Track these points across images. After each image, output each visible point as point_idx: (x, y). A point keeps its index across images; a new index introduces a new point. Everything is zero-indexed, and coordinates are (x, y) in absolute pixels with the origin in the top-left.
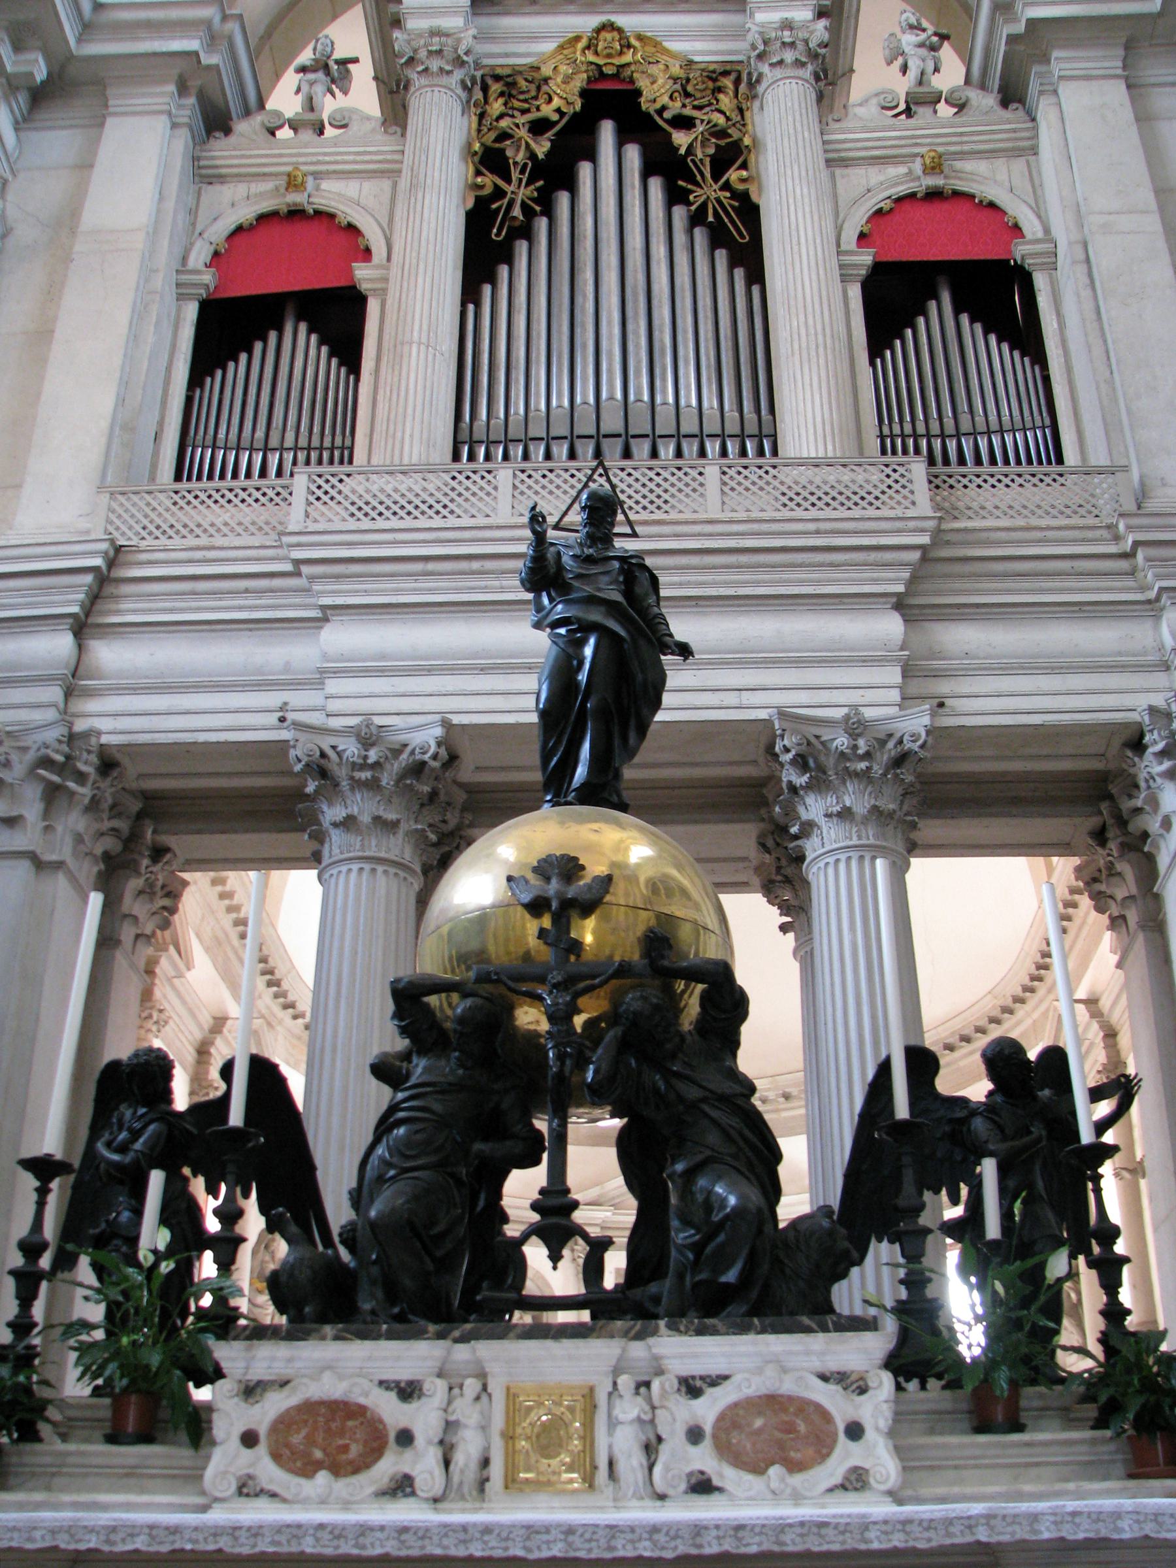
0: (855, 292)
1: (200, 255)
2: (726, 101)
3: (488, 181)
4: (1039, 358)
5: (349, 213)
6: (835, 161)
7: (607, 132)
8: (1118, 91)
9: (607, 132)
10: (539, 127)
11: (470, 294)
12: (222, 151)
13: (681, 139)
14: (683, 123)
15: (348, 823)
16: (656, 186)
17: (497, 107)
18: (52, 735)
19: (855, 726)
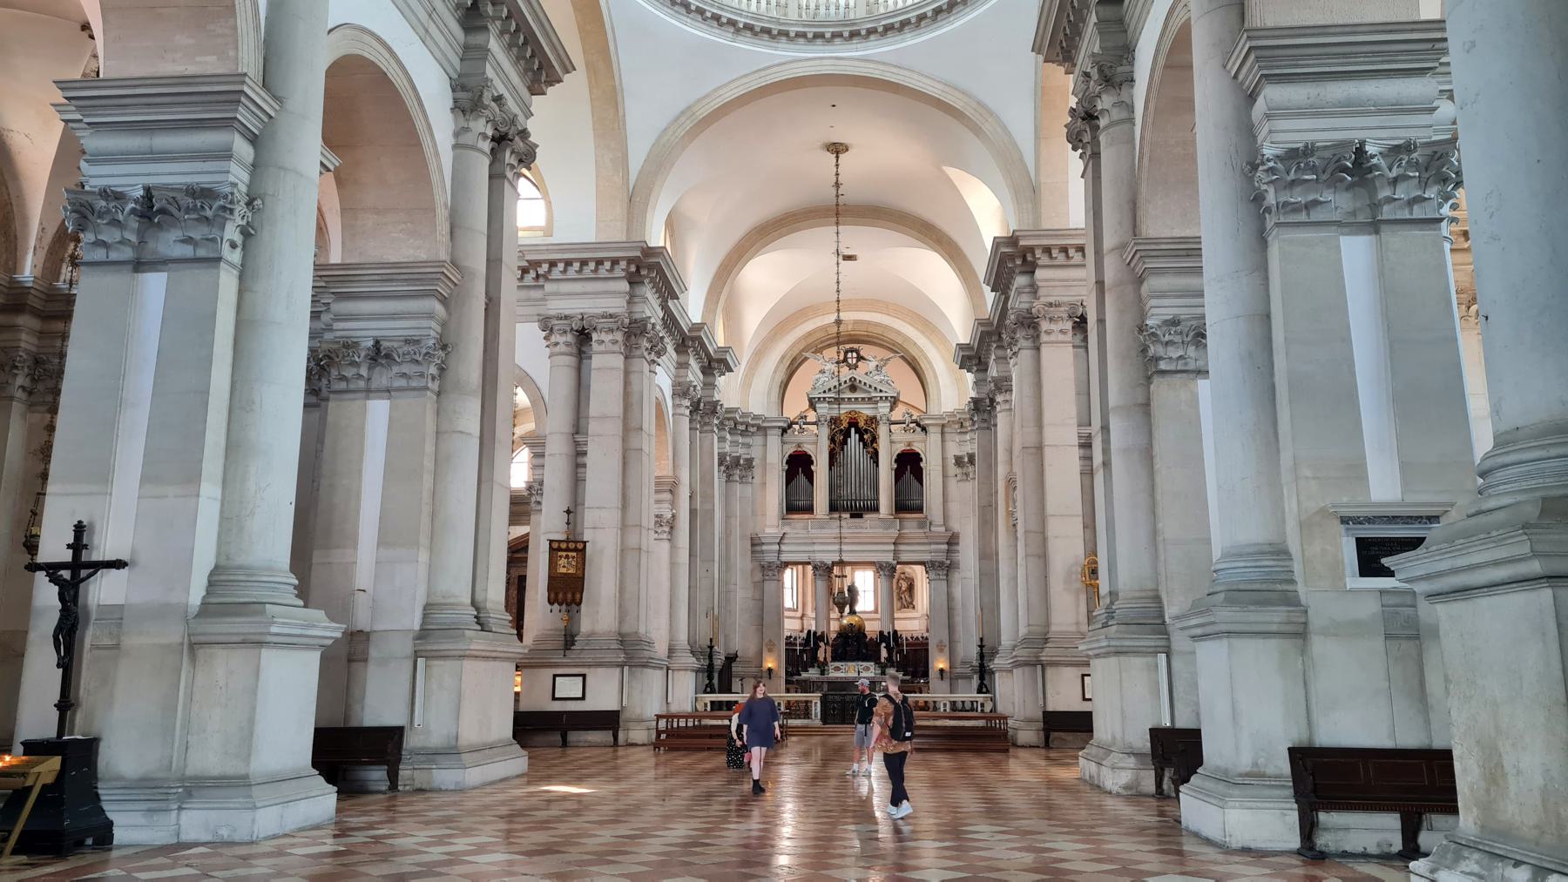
0: (893, 472)
2: (874, 426)
3: (832, 445)
4: (922, 484)
5: (810, 453)
6: (892, 442)
7: (853, 430)
8: (940, 435)
9: (853, 430)
10: (841, 430)
11: (830, 469)
13: (865, 437)
14: (866, 431)
15: (820, 575)
16: (861, 443)
17: (833, 427)
18: (779, 563)
19: (887, 563)
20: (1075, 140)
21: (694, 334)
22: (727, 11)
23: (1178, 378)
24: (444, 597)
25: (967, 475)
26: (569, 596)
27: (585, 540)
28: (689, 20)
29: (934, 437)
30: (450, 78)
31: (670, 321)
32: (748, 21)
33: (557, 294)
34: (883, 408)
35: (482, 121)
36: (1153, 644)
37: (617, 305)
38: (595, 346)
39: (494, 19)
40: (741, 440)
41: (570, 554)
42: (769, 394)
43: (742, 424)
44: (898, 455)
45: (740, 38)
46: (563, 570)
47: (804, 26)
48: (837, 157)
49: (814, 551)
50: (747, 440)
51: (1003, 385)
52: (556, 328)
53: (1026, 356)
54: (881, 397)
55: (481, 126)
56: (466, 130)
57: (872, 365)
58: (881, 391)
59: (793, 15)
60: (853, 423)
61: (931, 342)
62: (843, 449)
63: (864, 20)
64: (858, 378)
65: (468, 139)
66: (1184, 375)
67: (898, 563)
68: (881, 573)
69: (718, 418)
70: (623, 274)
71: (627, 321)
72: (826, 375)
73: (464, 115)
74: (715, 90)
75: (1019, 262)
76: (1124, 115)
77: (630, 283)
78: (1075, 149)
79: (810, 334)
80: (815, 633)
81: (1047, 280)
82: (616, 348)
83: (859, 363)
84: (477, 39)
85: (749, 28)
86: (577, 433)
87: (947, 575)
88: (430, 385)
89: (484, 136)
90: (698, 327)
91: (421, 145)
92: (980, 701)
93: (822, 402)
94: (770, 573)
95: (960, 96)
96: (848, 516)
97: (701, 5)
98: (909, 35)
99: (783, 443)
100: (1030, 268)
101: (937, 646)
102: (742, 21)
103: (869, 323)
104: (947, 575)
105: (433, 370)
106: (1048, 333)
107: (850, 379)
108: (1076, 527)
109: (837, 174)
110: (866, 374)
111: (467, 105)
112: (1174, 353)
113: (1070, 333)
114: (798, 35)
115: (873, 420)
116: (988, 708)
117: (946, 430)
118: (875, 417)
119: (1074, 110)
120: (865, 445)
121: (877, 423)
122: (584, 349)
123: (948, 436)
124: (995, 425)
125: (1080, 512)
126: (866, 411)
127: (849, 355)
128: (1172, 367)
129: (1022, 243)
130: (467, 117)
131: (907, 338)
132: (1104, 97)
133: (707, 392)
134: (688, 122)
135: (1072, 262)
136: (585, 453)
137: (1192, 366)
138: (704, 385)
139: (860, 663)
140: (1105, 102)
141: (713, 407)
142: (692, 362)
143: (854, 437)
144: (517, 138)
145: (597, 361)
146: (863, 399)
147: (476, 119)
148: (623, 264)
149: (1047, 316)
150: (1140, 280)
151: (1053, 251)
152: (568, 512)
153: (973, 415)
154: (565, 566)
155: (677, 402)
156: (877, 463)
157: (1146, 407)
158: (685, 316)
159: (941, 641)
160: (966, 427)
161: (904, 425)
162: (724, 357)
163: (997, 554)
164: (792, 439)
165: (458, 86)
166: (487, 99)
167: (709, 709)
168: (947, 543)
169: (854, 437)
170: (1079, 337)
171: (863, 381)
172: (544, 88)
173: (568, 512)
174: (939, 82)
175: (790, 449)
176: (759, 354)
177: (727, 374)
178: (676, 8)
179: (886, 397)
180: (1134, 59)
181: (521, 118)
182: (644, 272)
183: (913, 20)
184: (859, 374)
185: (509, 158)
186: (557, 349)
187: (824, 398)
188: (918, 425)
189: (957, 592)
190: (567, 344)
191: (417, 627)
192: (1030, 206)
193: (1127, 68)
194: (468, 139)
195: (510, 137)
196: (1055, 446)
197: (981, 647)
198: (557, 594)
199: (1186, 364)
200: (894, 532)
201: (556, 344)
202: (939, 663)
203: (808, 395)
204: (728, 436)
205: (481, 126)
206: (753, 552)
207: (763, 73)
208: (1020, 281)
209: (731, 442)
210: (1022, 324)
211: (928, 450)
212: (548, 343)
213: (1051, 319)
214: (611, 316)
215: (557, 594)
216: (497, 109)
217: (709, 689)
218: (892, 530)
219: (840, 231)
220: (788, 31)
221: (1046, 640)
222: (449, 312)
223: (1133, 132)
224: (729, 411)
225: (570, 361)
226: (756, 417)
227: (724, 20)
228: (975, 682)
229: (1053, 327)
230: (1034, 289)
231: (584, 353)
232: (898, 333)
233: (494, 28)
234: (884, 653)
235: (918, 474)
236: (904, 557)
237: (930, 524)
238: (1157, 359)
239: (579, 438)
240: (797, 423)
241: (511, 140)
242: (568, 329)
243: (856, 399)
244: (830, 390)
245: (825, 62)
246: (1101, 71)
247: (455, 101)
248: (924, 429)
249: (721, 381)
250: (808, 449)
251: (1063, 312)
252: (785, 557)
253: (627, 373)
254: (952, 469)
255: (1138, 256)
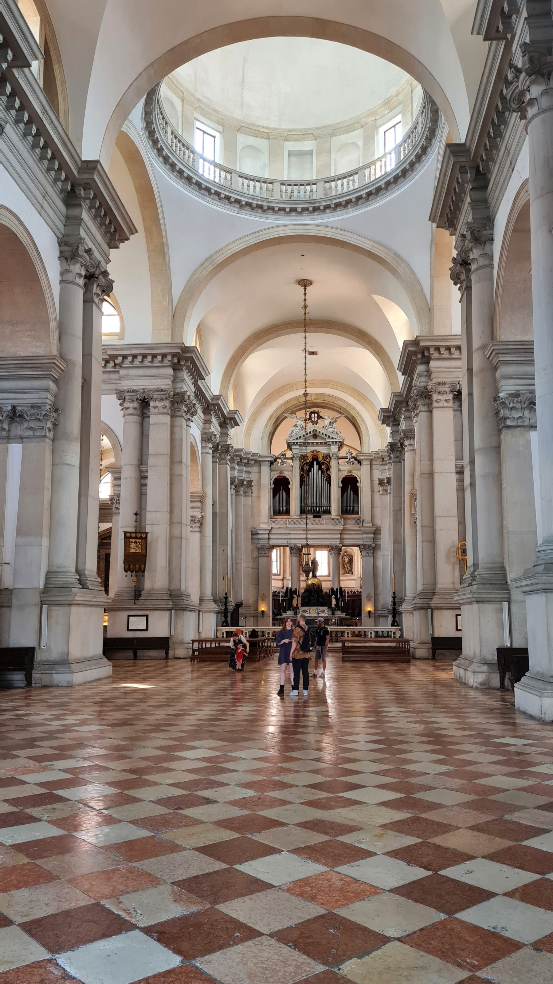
1: (272, 482)
2: (328, 460)
4: (358, 497)
5: (288, 477)
6: (339, 470)
7: (315, 463)
8: (369, 466)
9: (315, 463)
11: (301, 487)
12: (273, 467)
13: (323, 467)
14: (323, 463)
16: (320, 471)
18: (268, 546)
20: (456, 278)
21: (215, 402)
22: (234, 194)
23: (517, 431)
24: (58, 567)
25: (386, 491)
26: (137, 566)
27: (147, 531)
28: (210, 200)
29: (366, 467)
30: (58, 238)
31: (200, 394)
32: (248, 200)
33: (127, 376)
34: (334, 449)
35: (78, 266)
36: (499, 596)
37: (165, 384)
38: (152, 410)
39: (85, 199)
40: (244, 469)
41: (138, 540)
42: (262, 439)
43: (245, 459)
44: (343, 478)
45: (243, 211)
46: (134, 551)
47: (284, 203)
48: (305, 289)
49: (290, 539)
50: (249, 469)
51: (409, 434)
52: (127, 398)
53: (423, 416)
54: (333, 442)
55: (77, 268)
56: (68, 271)
57: (327, 422)
58: (332, 438)
59: (277, 196)
60: (315, 459)
61: (365, 407)
62: (308, 475)
63: (322, 200)
64: (318, 430)
65: (69, 277)
66: (522, 428)
67: (343, 546)
68: (332, 552)
69: (230, 455)
70: (169, 364)
71: (172, 394)
72: (298, 428)
73: (67, 261)
74: (228, 245)
75: (419, 356)
76: (487, 262)
77: (174, 370)
78: (455, 284)
79: (288, 402)
80: (291, 589)
81: (437, 368)
82: (165, 411)
83: (319, 421)
84: (75, 212)
85: (248, 204)
86: (141, 464)
87: (373, 553)
88: (48, 434)
89: (80, 275)
90: (217, 398)
91: (39, 281)
92: (393, 631)
93: (295, 445)
94: (263, 552)
95: (382, 249)
96: (312, 516)
97: (218, 190)
98: (351, 210)
99: (271, 471)
100: (427, 360)
101: (367, 597)
102: (244, 200)
103: (325, 395)
104: (373, 553)
105: (49, 425)
106: (437, 401)
107: (313, 431)
108: (453, 523)
109: (305, 300)
110: (323, 427)
111: (68, 254)
112: (516, 414)
113: (451, 402)
114: (281, 209)
115: (327, 457)
116: (398, 635)
117: (374, 462)
118: (329, 455)
119: (455, 259)
120: (322, 472)
121: (330, 458)
122: (145, 411)
123: (374, 467)
124: (404, 460)
125: (456, 514)
126: (323, 450)
127: (313, 415)
128: (514, 423)
129: (422, 344)
130: (69, 262)
131: (349, 405)
132: (474, 250)
133: (223, 439)
134: (210, 266)
135: (453, 356)
136: (146, 477)
137: (527, 423)
138: (221, 434)
139: (319, 608)
140: (475, 254)
141: (227, 448)
142: (213, 419)
143: (316, 467)
144: (101, 277)
145: (153, 419)
146: (321, 443)
147: (74, 264)
148: (169, 357)
149: (437, 391)
150: (495, 369)
151: (441, 350)
152: (136, 514)
153: (390, 453)
154: (134, 548)
155: (204, 445)
156: (330, 483)
157: (497, 448)
158: (208, 390)
159: (369, 594)
160: (386, 461)
161: (347, 460)
162: (233, 417)
163: (404, 540)
164: (277, 468)
165: (63, 242)
166: (81, 252)
167: (225, 636)
168: (374, 534)
169: (316, 467)
170: (457, 404)
171: (321, 432)
172: (118, 244)
173: (136, 514)
174: (370, 240)
175: (275, 475)
176: (256, 415)
177: (236, 427)
178: (202, 191)
179: (336, 442)
180: (493, 226)
181: (103, 263)
182: (183, 363)
183: (354, 200)
184: (319, 428)
185: (95, 289)
186: (128, 411)
187: (297, 443)
188: (356, 459)
189: (379, 563)
190: (134, 408)
191: (42, 586)
192: (427, 320)
193: (489, 232)
194: (69, 277)
195: (96, 276)
196: (441, 472)
197: (394, 597)
198: (129, 566)
199: (523, 422)
200: (340, 527)
201: (128, 408)
202: (368, 607)
203: (287, 441)
204: (237, 467)
205: (77, 268)
206: (252, 539)
207: (257, 234)
208: (420, 368)
209: (238, 470)
210: (421, 396)
211: (362, 475)
212: (122, 408)
213: (439, 393)
214: (162, 391)
215: (129, 566)
216: (88, 258)
217: (225, 624)
218: (339, 526)
219: (307, 336)
220: (274, 207)
221: (434, 594)
222: (59, 389)
223: (492, 273)
224: (237, 450)
225: (136, 419)
226: (254, 455)
227: (233, 200)
228: (390, 619)
229: (441, 397)
230: (429, 373)
231: (145, 414)
232: (344, 401)
233: (85, 205)
234: (334, 602)
235: (356, 490)
236: (347, 542)
237: (363, 521)
238: (505, 418)
239: (142, 468)
240: (279, 458)
241: (97, 278)
242: (135, 399)
243: (317, 443)
244: (300, 437)
245: (297, 227)
246: (472, 233)
247: (61, 252)
248: (359, 462)
249: (232, 432)
250: (287, 474)
251: (447, 388)
252: (272, 542)
253: (172, 427)
254: (377, 487)
255: (494, 353)
